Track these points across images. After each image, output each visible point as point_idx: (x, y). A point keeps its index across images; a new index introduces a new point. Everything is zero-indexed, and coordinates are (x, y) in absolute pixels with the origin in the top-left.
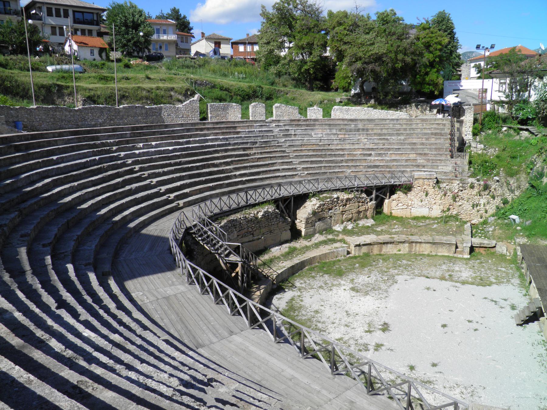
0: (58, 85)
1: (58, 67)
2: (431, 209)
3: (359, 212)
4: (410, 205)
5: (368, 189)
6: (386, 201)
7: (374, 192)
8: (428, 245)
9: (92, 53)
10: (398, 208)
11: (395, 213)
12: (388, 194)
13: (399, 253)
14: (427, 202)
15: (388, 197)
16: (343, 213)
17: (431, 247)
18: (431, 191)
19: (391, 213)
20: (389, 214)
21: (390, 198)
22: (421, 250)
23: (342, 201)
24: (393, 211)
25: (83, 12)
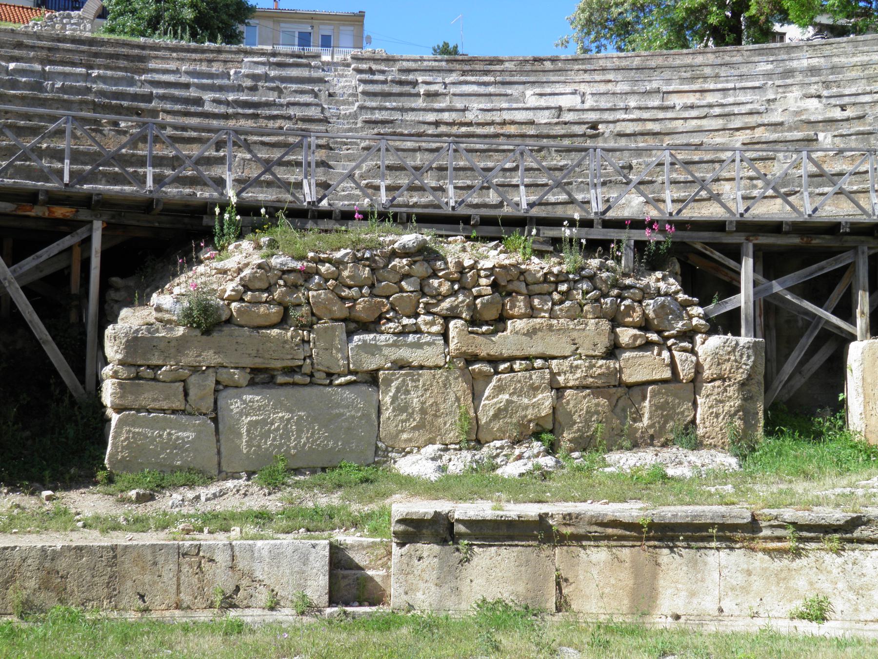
3: (622, 393)
5: (697, 240)
6: (856, 352)
7: (747, 268)
12: (863, 302)
15: (862, 322)
23: (462, 279)
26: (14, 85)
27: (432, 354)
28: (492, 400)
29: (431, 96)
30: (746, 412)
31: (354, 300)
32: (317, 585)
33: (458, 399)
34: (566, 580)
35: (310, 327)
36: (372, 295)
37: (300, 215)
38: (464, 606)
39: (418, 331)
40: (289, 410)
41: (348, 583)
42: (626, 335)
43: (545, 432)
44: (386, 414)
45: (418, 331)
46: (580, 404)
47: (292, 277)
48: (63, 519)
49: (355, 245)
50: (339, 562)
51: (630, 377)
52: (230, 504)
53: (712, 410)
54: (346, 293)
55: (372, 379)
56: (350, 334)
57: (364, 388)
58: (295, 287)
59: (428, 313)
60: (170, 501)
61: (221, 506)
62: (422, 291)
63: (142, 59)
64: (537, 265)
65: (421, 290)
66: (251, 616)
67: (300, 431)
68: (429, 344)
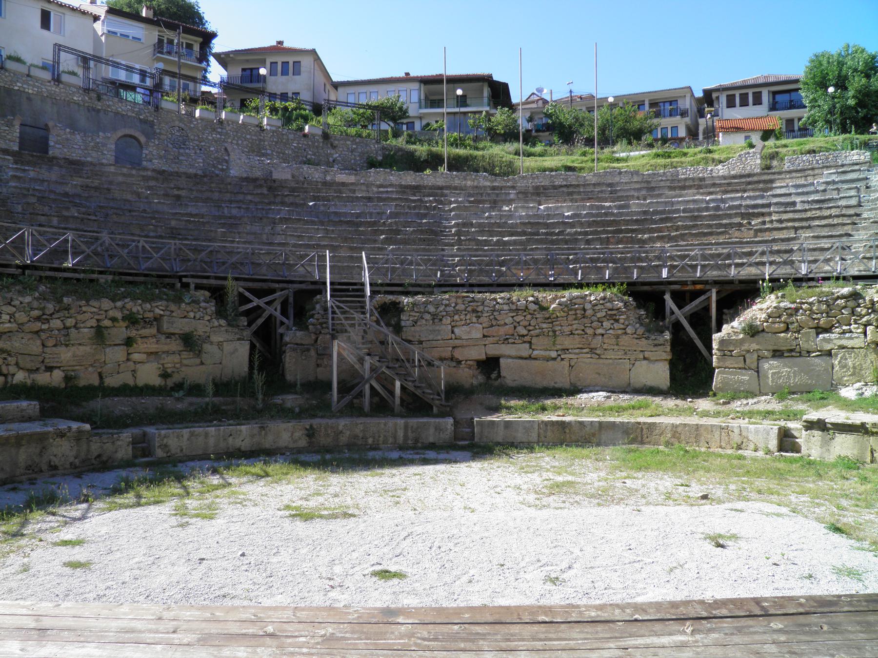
26: (707, 209)
27: (858, 342)
31: (819, 319)
32: (773, 444)
33: (872, 362)
34: (684, 456)
35: (798, 332)
36: (828, 316)
37: (799, 281)
38: (831, 458)
39: (851, 332)
40: (789, 367)
41: (786, 441)
44: (837, 368)
45: (851, 332)
47: (789, 311)
48: (693, 411)
49: (819, 296)
52: (762, 407)
54: (815, 316)
55: (829, 354)
56: (818, 334)
57: (824, 357)
58: (791, 315)
59: (856, 323)
61: (756, 407)
62: (853, 313)
65: (853, 312)
67: (795, 377)
68: (856, 337)
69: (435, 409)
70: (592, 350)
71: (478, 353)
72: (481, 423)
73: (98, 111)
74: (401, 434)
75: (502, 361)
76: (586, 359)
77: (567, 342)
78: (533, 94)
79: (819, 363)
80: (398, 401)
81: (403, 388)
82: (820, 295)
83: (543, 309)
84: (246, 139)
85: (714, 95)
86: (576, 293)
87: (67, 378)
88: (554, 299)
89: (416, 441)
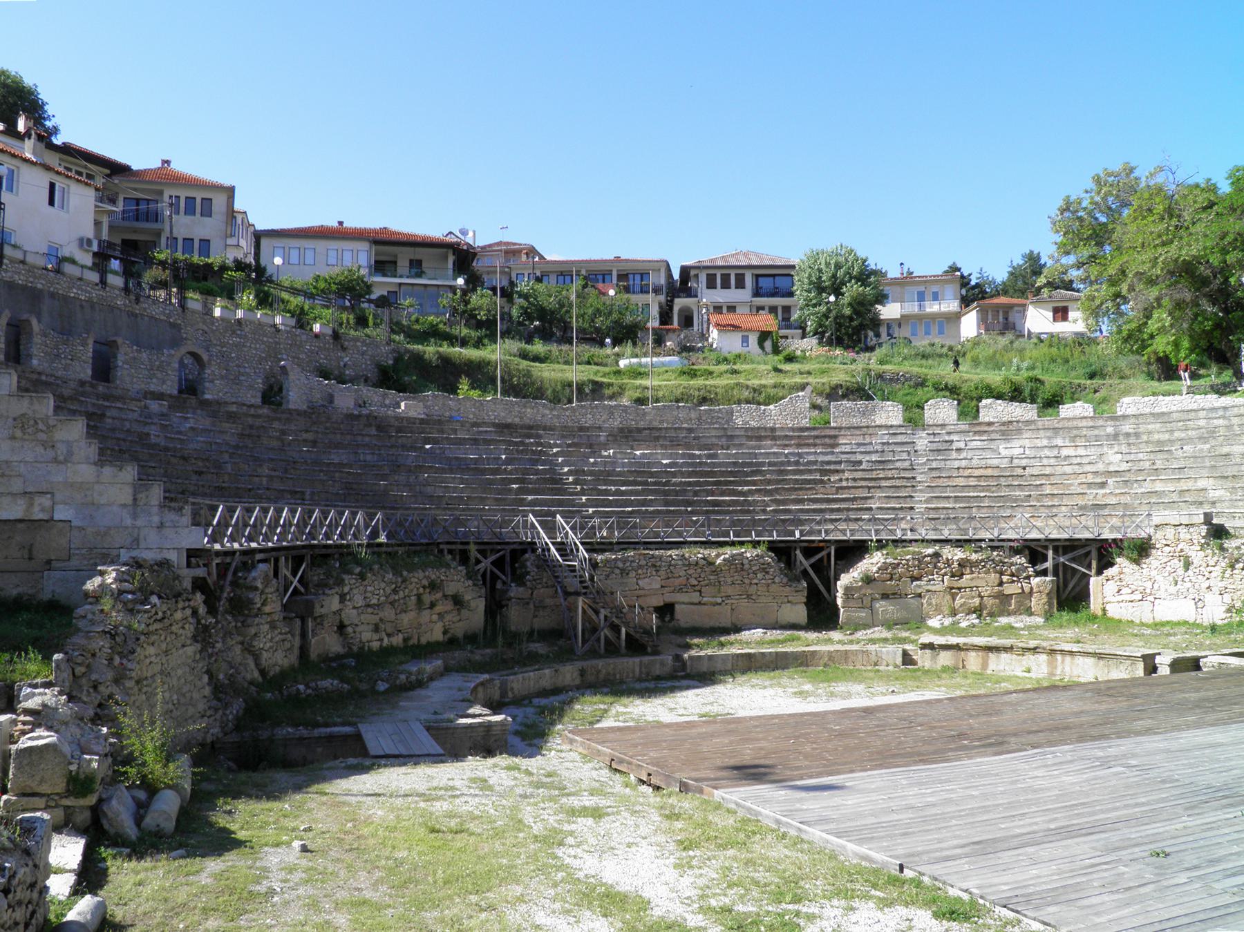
0: (595, 383)
1: (634, 360)
2: (1200, 604)
3: (1004, 598)
4: (1148, 591)
5: (1033, 545)
6: (1092, 580)
7: (1050, 553)
8: (1090, 661)
9: (745, 340)
10: (1120, 598)
11: (1114, 611)
13: (1027, 675)
14: (1188, 585)
15: (1094, 571)
16: (952, 592)
17: (1097, 665)
18: (1197, 557)
19: (1104, 610)
20: (1100, 613)
21: (1099, 572)
22: (1075, 673)
23: (948, 563)
24: (1108, 607)
25: (774, 276)
26: (789, 463)
27: (938, 588)
28: (959, 601)
29: (959, 450)
30: (1050, 604)
32: (899, 660)
41: (907, 659)
42: (1005, 578)
43: (978, 611)
46: (989, 602)
48: (830, 641)
50: (905, 654)
51: (1006, 592)
53: (1037, 603)
55: (920, 595)
60: (860, 634)
61: (873, 636)
62: (935, 567)
63: (835, 437)
64: (974, 557)
66: (881, 668)
69: (649, 649)
70: (749, 597)
71: (658, 601)
72: (691, 658)
73: (136, 316)
74: (637, 670)
75: (677, 606)
76: (744, 602)
77: (730, 591)
78: (451, 233)
79: (914, 602)
80: (623, 644)
81: (627, 634)
82: (914, 553)
83: (712, 564)
84: (264, 343)
85: (693, 273)
86: (736, 551)
87: (405, 640)
88: (718, 556)
89: (648, 674)
